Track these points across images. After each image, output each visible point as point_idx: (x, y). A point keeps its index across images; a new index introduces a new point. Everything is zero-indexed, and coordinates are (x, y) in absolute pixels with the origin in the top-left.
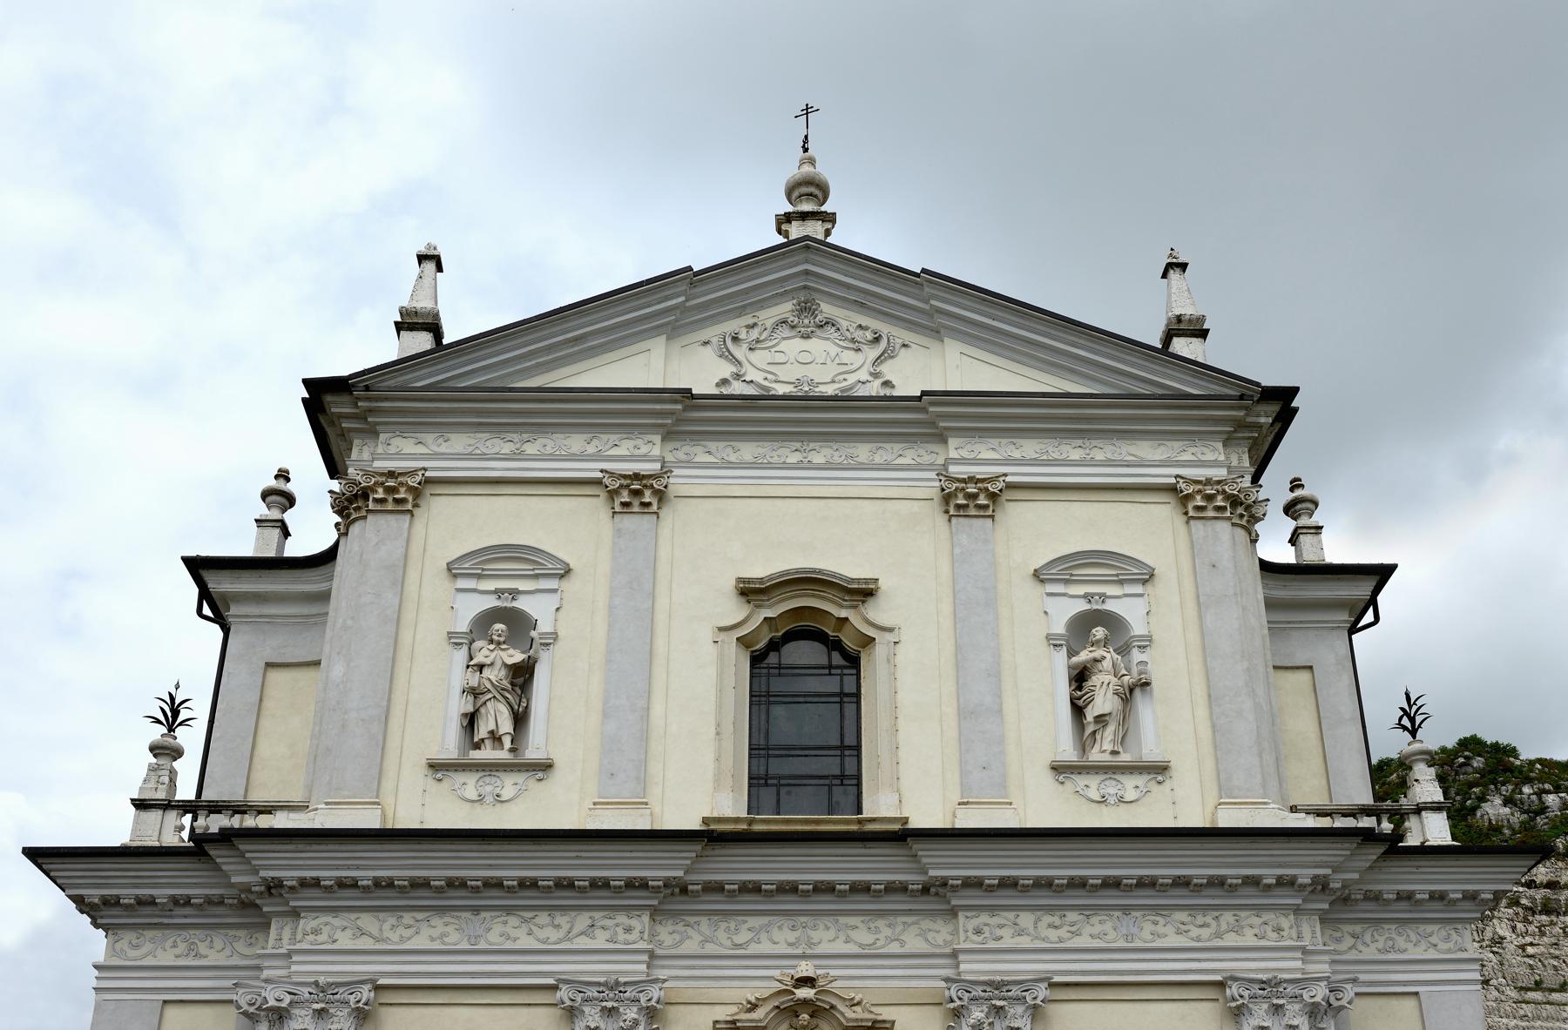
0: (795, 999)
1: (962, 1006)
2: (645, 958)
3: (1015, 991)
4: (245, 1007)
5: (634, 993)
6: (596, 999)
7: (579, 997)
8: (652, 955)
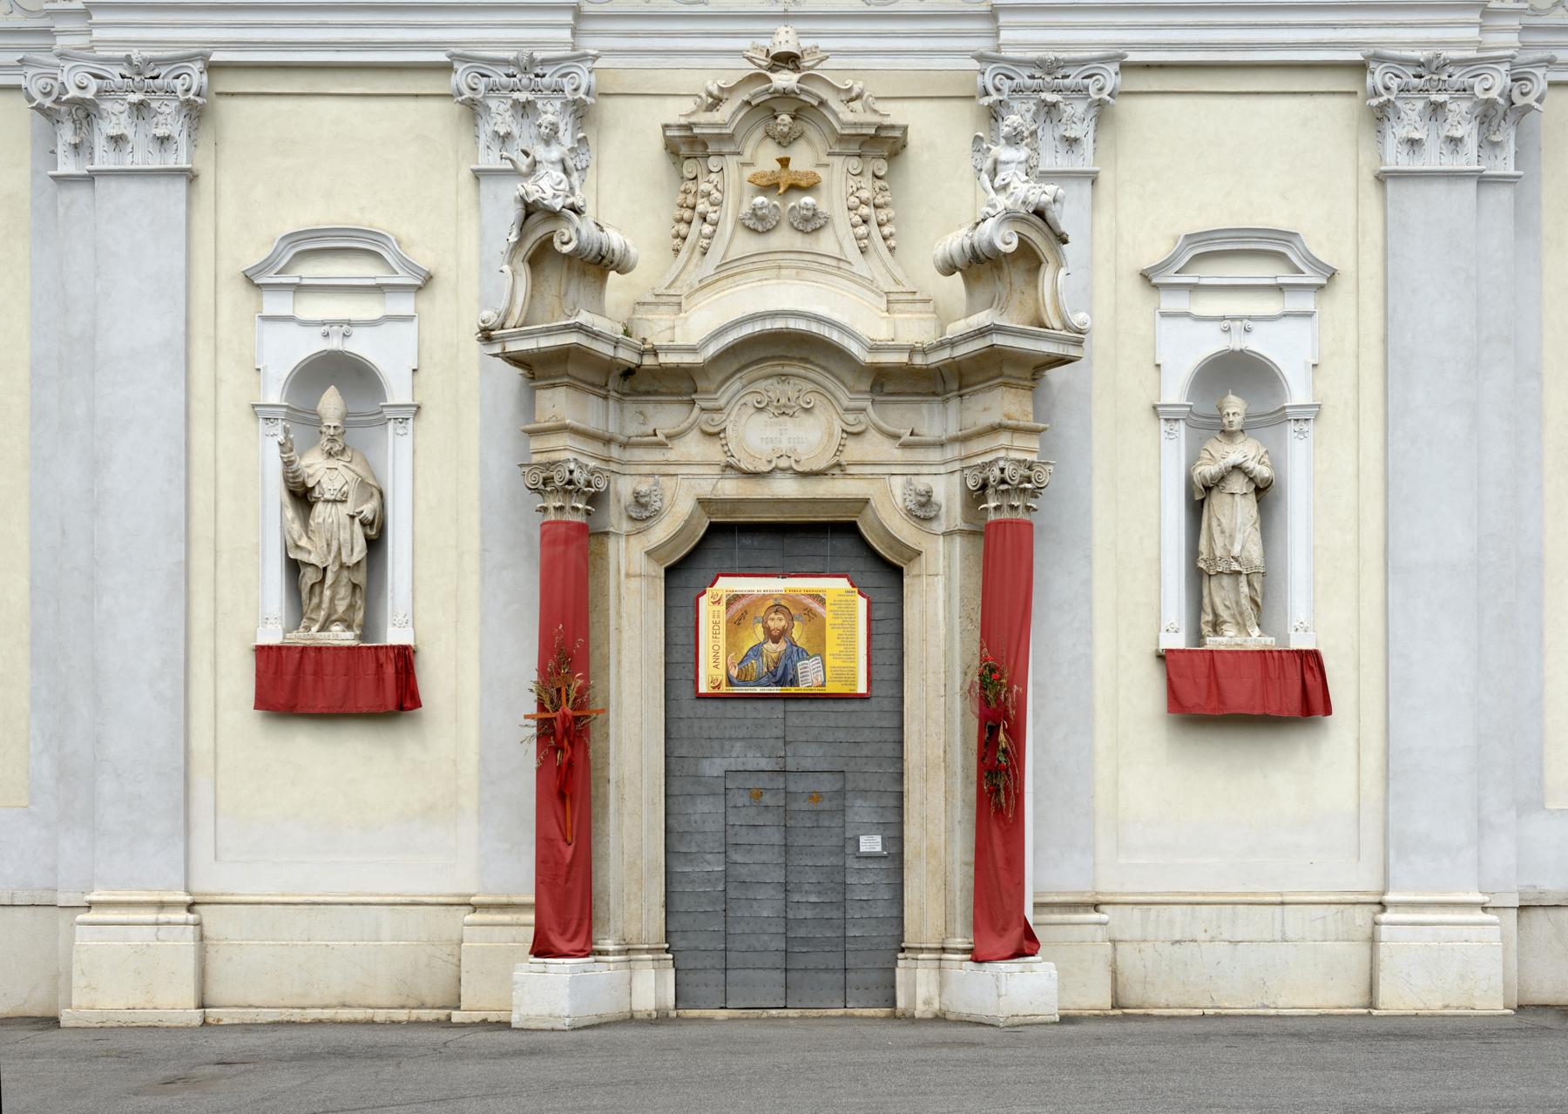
0: (772, 90)
1: (1001, 101)
2: (568, 18)
3: (1075, 78)
4: (39, 99)
5: (555, 78)
6: (505, 88)
7: (482, 84)
8: (579, 14)
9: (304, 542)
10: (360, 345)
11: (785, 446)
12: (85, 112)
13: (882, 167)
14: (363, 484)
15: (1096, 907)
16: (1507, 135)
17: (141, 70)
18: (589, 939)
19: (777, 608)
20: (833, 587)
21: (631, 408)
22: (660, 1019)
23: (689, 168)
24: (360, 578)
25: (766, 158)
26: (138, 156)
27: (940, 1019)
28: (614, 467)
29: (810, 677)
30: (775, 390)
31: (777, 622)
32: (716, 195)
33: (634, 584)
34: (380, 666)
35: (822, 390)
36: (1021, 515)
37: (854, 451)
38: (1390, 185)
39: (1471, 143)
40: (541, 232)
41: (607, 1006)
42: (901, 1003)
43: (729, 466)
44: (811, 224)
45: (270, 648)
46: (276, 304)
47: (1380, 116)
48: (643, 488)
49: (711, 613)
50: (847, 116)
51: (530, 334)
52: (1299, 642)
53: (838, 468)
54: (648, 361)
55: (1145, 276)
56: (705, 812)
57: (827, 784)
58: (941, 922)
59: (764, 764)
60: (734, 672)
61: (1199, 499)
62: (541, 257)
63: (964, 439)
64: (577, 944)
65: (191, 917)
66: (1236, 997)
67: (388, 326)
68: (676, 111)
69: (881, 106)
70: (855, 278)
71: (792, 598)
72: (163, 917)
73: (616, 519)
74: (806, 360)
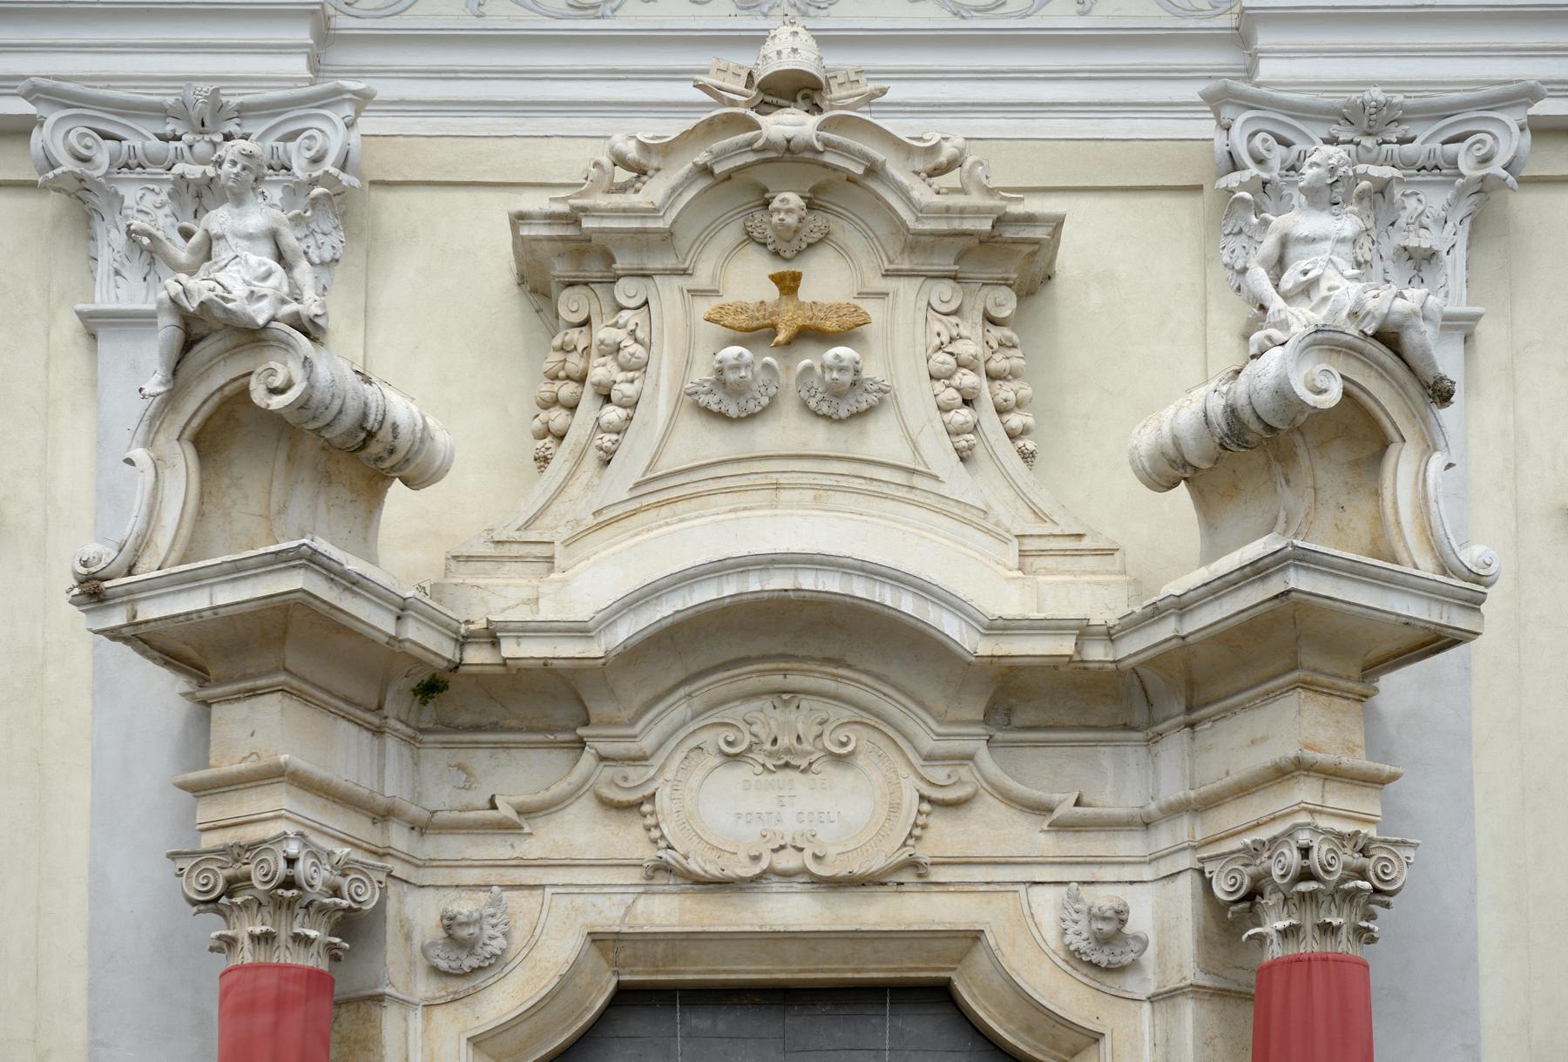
11: (789, 828)
21: (436, 759)
30: (767, 720)
35: (874, 720)
43: (662, 868)
48: (465, 906)
70: (948, 508)
74: (839, 662)
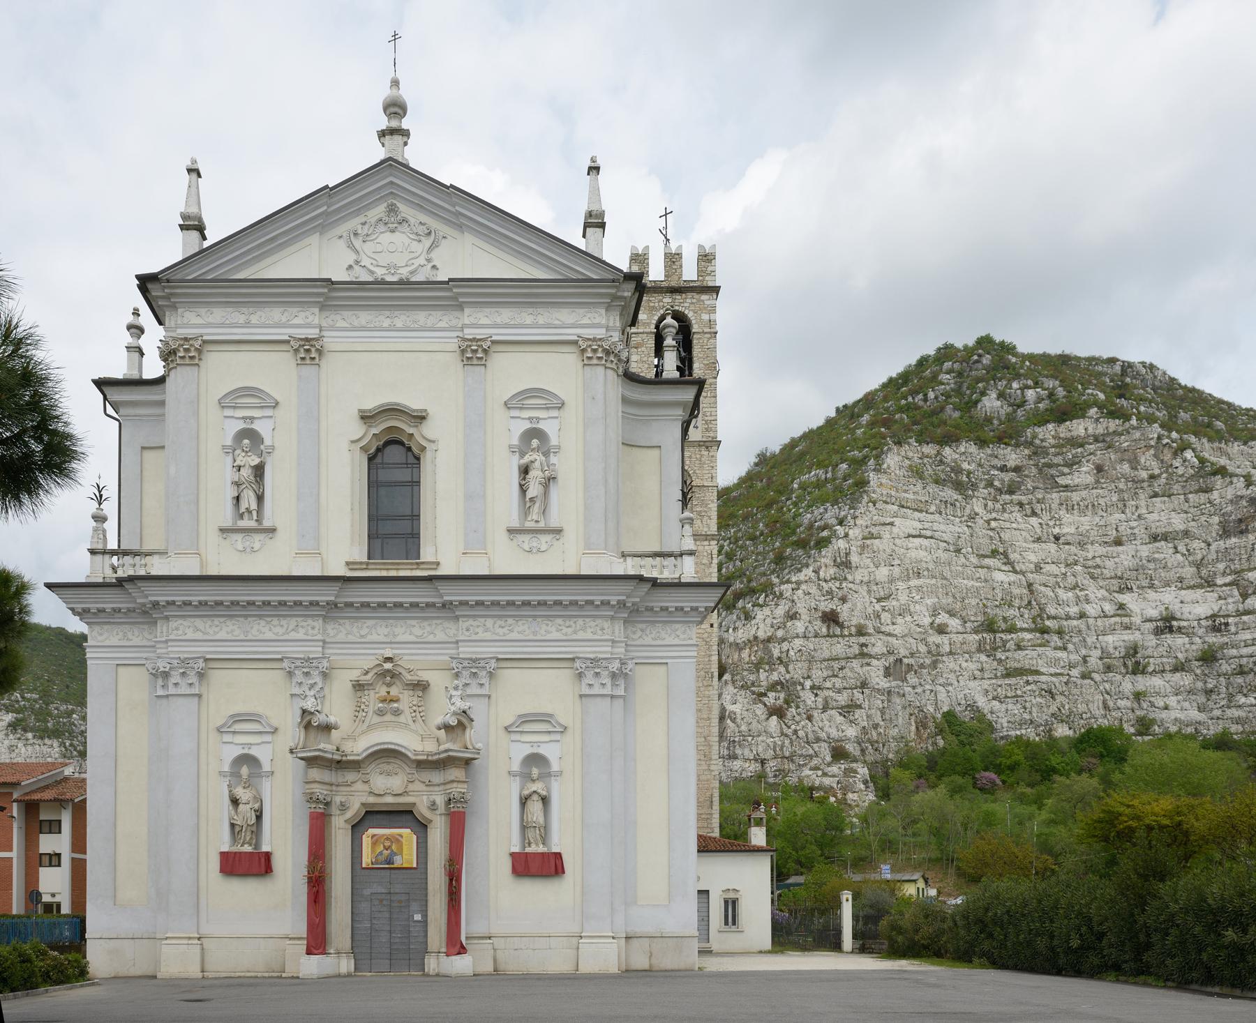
2: (321, 644)
3: (482, 664)
4: (151, 671)
7: (293, 666)
8: (324, 642)
9: (235, 817)
10: (254, 751)
11: (389, 786)
12: (166, 675)
13: (420, 694)
14: (255, 797)
15: (490, 938)
16: (621, 682)
17: (183, 661)
18: (324, 949)
19: (387, 839)
20: (406, 832)
21: (340, 773)
22: (349, 975)
23: (359, 694)
24: (254, 829)
25: (383, 691)
26: (183, 690)
27: (437, 975)
28: (334, 793)
29: (398, 861)
30: (386, 767)
31: (387, 844)
32: (367, 703)
33: (341, 831)
34: (260, 859)
35: (400, 768)
36: (461, 809)
37: (411, 787)
38: (583, 699)
39: (609, 685)
40: (308, 718)
41: (330, 971)
42: (426, 970)
43: (371, 792)
44: (397, 712)
45: (224, 852)
46: (227, 738)
47: (580, 675)
48: (343, 800)
49: (366, 841)
50: (410, 678)
51: (304, 751)
52: (555, 850)
53: (405, 793)
54: (344, 758)
55: (506, 728)
56: (364, 907)
57: (404, 897)
58: (438, 944)
59: (384, 891)
60: (374, 860)
61: (524, 801)
62: (308, 726)
63: (445, 784)
64: (320, 951)
65: (199, 942)
66: (535, 968)
67: (263, 745)
68: (355, 675)
69: (419, 673)
70: (411, 730)
71: (392, 836)
72: (190, 942)
73: (334, 810)
74: (395, 757)
